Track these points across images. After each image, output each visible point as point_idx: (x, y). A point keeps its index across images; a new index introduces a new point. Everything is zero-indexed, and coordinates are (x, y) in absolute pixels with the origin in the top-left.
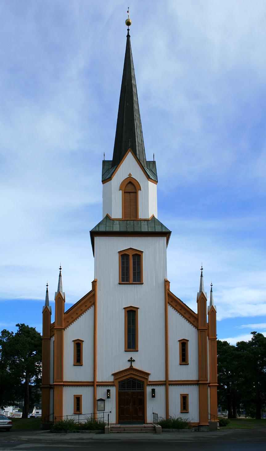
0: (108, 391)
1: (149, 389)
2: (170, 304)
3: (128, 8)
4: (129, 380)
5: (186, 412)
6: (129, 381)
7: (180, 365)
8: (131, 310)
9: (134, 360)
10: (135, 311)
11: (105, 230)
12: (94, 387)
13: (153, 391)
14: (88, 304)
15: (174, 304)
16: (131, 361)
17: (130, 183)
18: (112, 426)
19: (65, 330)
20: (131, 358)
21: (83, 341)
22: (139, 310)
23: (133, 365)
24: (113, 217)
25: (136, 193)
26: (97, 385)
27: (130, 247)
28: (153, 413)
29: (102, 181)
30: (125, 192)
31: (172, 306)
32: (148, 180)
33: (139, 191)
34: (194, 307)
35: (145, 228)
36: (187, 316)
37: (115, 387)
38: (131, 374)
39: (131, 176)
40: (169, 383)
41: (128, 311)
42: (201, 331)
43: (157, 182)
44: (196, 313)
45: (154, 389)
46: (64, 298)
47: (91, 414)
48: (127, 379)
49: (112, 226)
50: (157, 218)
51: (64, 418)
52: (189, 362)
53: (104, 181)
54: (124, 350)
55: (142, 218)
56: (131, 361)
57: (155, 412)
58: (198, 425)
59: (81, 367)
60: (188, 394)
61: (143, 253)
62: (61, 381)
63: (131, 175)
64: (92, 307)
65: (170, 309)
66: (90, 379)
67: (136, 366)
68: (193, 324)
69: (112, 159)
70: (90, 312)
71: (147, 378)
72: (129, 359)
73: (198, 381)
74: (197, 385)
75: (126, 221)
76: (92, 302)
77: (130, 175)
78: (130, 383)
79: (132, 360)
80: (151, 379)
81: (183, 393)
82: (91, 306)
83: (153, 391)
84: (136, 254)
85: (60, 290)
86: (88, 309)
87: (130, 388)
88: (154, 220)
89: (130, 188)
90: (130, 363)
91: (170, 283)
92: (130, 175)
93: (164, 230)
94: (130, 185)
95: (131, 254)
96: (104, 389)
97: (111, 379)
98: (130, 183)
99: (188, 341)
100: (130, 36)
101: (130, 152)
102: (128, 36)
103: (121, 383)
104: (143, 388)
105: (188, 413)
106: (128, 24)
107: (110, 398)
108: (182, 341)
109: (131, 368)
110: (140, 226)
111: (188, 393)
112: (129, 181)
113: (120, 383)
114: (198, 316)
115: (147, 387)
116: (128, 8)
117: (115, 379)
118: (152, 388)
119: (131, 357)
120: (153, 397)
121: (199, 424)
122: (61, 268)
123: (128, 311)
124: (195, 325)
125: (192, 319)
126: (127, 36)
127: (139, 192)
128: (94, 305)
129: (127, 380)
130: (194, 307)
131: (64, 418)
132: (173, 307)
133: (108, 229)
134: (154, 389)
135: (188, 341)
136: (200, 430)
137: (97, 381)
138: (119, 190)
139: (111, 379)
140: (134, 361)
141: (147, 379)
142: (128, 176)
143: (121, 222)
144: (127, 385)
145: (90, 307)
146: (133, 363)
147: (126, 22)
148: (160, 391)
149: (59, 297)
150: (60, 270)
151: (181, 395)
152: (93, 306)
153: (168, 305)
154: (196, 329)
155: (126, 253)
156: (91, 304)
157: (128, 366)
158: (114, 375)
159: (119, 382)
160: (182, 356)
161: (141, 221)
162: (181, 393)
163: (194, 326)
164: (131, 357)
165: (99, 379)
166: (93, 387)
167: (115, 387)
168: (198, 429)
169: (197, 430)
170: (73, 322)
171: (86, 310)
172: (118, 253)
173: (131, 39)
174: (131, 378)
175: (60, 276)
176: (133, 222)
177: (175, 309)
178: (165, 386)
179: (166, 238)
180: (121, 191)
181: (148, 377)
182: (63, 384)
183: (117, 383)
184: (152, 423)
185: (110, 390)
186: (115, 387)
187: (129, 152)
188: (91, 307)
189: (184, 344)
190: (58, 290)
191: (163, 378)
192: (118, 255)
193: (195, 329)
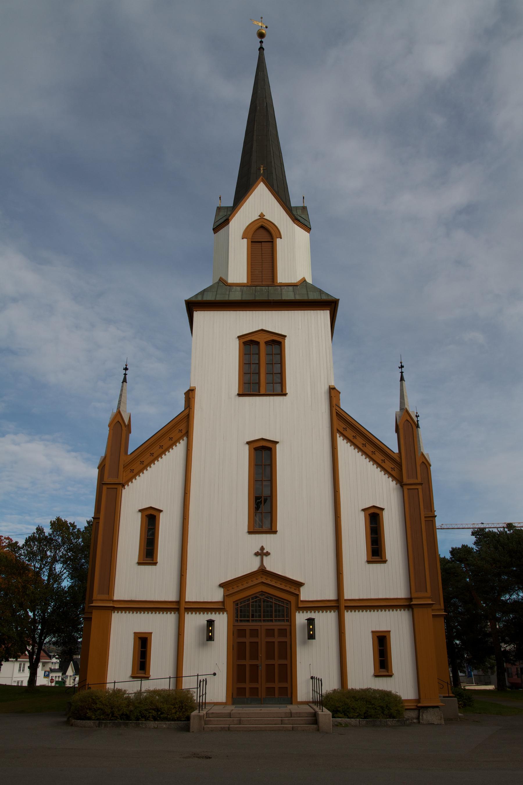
0: (211, 623)
1: (301, 618)
2: (342, 434)
3: (262, 18)
4: (256, 597)
5: (387, 674)
6: (256, 602)
7: (369, 562)
9: (267, 552)
10: (270, 449)
11: (214, 299)
12: (179, 613)
13: (311, 621)
15: (350, 433)
16: (262, 553)
17: (262, 227)
18: (216, 710)
19: (124, 488)
20: (262, 548)
21: (161, 511)
22: (278, 446)
23: (265, 564)
24: (230, 280)
25: (272, 243)
26: (185, 608)
27: (260, 328)
28: (312, 678)
29: (213, 229)
30: (252, 242)
31: (345, 437)
32: (294, 222)
33: (277, 239)
35: (289, 295)
36: (379, 457)
38: (263, 582)
39: (264, 217)
40: (347, 605)
41: (256, 449)
42: (408, 489)
43: (310, 229)
45: (313, 620)
46: (127, 422)
47: (170, 678)
48: (255, 597)
49: (228, 293)
50: (311, 283)
51: (110, 686)
52: (388, 556)
53: (216, 229)
54: (246, 529)
55: (283, 282)
56: (262, 553)
57: (315, 675)
58: (417, 706)
59: (154, 567)
60: (389, 632)
62: (107, 599)
63: (264, 216)
64: (183, 440)
65: (341, 442)
66: (171, 596)
67: (271, 565)
68: (390, 475)
69: (232, 206)
70: (179, 449)
73: (410, 599)
74: (408, 610)
75: (254, 287)
76: (184, 431)
77: (262, 216)
78: (260, 606)
79: (265, 551)
80: (305, 595)
81: (378, 629)
82: (181, 438)
85: (121, 407)
86: (174, 444)
87: (260, 616)
88: (306, 286)
89: (263, 236)
90: (259, 558)
91: (340, 393)
92: (262, 216)
93: (324, 298)
94: (262, 231)
95: (262, 339)
96: (201, 619)
97: (218, 596)
98: (262, 227)
99: (383, 509)
100: (264, 49)
101: (262, 183)
102: (261, 49)
103: (239, 605)
104: (287, 616)
105: (391, 676)
106: (261, 35)
107: (214, 640)
108: (372, 511)
109: (262, 571)
110: (280, 293)
111: (388, 629)
112: (260, 224)
113: (237, 605)
114: (400, 458)
115: (297, 614)
116: (262, 18)
117: (227, 596)
119: (262, 547)
120: (312, 637)
121: (419, 705)
122: (127, 367)
123: (256, 449)
124: (394, 475)
125: (388, 465)
126: (259, 49)
127: (278, 240)
128: (187, 437)
129: (252, 598)
131: (110, 686)
132: (349, 440)
133: (219, 298)
134: (313, 620)
135: (383, 509)
136: (421, 721)
137: (187, 600)
138: (243, 239)
139: (218, 596)
140: (268, 554)
141: (297, 596)
142: (259, 217)
143: (245, 288)
144: (252, 610)
145: (178, 441)
147: (259, 32)
149: (118, 421)
150: (124, 371)
151: (373, 632)
152: (185, 438)
153: (338, 435)
154: (398, 485)
156: (180, 434)
157: (253, 565)
159: (236, 603)
160: (372, 545)
161: (282, 287)
162: (374, 630)
163: (394, 478)
164: (262, 547)
165: (191, 596)
166: (177, 613)
167: (225, 613)
168: (418, 718)
169: (415, 721)
170: (142, 471)
171: (171, 447)
172: (238, 339)
173: (265, 52)
174: (262, 593)
176: (267, 288)
177: (353, 443)
178: (337, 611)
179: (328, 312)
180: (245, 240)
181: (299, 591)
182: (111, 605)
184: (310, 702)
185: (214, 621)
186: (225, 613)
187: (260, 183)
188: (181, 441)
190: (119, 408)
191: (330, 595)
192: (237, 341)
193: (396, 484)
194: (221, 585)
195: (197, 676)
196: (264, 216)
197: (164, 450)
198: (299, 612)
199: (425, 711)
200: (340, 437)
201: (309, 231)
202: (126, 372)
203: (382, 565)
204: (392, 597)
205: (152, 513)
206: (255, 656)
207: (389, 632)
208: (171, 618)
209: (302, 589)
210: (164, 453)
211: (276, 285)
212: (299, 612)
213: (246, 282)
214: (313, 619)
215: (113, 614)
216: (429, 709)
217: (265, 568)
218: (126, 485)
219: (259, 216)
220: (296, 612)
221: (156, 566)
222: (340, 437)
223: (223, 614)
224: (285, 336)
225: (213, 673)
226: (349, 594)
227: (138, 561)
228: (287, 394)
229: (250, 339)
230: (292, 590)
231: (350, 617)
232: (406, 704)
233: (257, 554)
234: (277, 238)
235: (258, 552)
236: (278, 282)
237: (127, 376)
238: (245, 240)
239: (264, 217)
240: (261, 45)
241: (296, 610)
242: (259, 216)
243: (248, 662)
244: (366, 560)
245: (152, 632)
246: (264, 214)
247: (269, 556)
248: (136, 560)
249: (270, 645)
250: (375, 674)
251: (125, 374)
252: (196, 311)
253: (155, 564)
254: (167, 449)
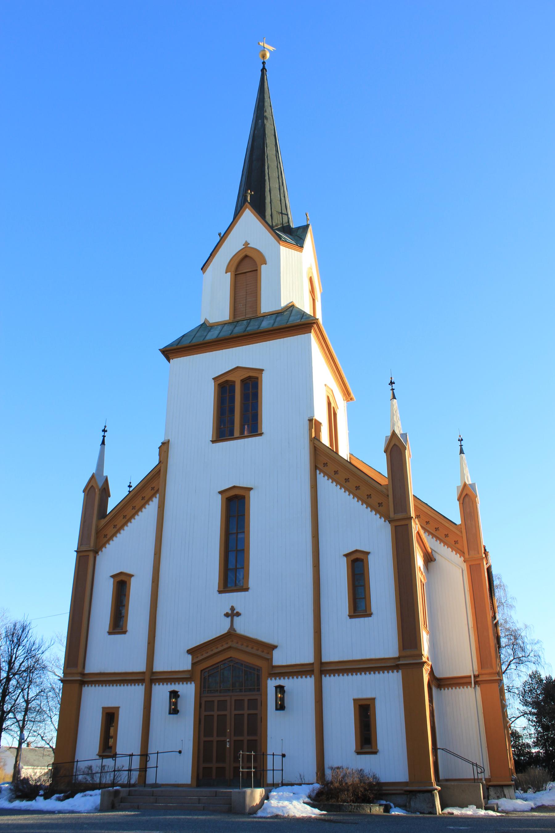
8: (236, 497)
9: (237, 613)
13: (280, 689)
14: (148, 492)
16: (233, 614)
17: (246, 256)
20: (232, 609)
22: (252, 493)
31: (325, 474)
37: (193, 685)
38: (230, 647)
39: (249, 246)
56: (233, 614)
61: (264, 372)
63: (249, 244)
70: (152, 508)
71: (268, 657)
72: (237, 610)
73: (398, 658)
77: (247, 244)
79: (235, 612)
82: (154, 495)
83: (280, 689)
84: (250, 378)
86: (147, 502)
92: (247, 244)
98: (246, 256)
111: (373, 696)
118: (277, 684)
120: (281, 707)
132: (329, 477)
135: (368, 553)
138: (226, 273)
140: (238, 614)
141: (270, 660)
142: (244, 246)
145: (150, 499)
151: (354, 700)
155: (229, 378)
158: (190, 652)
162: (356, 697)
165: (159, 666)
171: (143, 506)
175: (103, 443)
180: (229, 274)
183: (198, 675)
186: (193, 683)
194: (190, 652)
195: (157, 754)
196: (249, 244)
197: (137, 510)
198: (271, 679)
199: (414, 797)
200: (320, 473)
201: (301, 250)
202: (104, 434)
203: (366, 619)
204: (378, 656)
205: (123, 579)
206: (222, 732)
208: (138, 690)
209: (275, 653)
210: (136, 513)
211: (259, 316)
212: (271, 679)
213: (228, 319)
215: (83, 687)
216: (419, 794)
217: (235, 631)
218: (99, 551)
219: (243, 245)
220: (268, 679)
221: (126, 635)
222: (320, 473)
223: (191, 683)
224: (262, 370)
225: (178, 751)
226: (329, 656)
227: (109, 630)
228: (263, 433)
229: (225, 380)
230: (264, 655)
231: (329, 681)
232: (384, 788)
233: (227, 615)
234: (262, 265)
235: (227, 613)
236: (262, 312)
237: (105, 438)
238: (229, 274)
239: (249, 246)
240: (264, 67)
241: (268, 677)
242: (243, 245)
243: (215, 738)
244: (348, 613)
245: (119, 706)
246: (249, 242)
247: (239, 617)
248: (107, 629)
249: (238, 719)
250: (357, 751)
251: (104, 436)
252: (173, 359)
253: (125, 632)
254: (140, 509)
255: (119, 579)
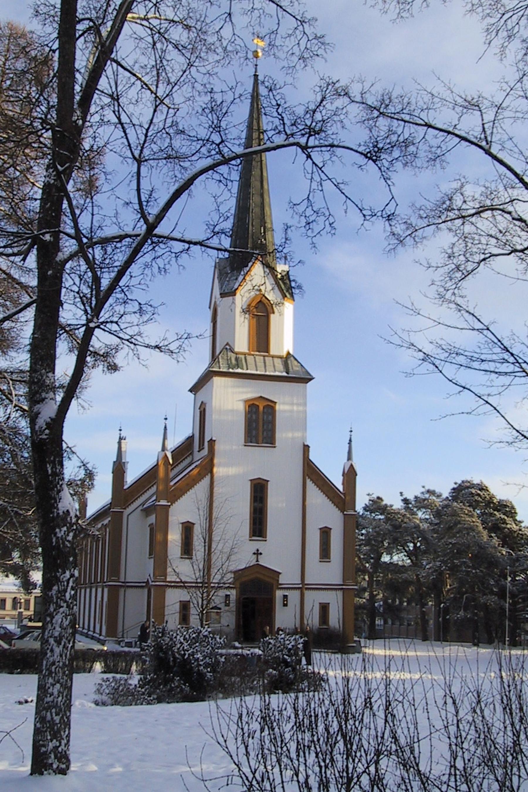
1: (279, 594)
2: (309, 478)
16: (257, 553)
25: (268, 318)
31: (311, 480)
34: (338, 482)
44: (341, 488)
56: (257, 553)
65: (309, 483)
80: (282, 580)
83: (285, 597)
90: (256, 556)
99: (331, 529)
120: (285, 605)
127: (272, 316)
130: (338, 482)
140: (261, 554)
146: (259, 556)
148: (294, 596)
152: (209, 474)
189: (325, 532)
207: (329, 604)
214: (287, 596)
255: (185, 525)
